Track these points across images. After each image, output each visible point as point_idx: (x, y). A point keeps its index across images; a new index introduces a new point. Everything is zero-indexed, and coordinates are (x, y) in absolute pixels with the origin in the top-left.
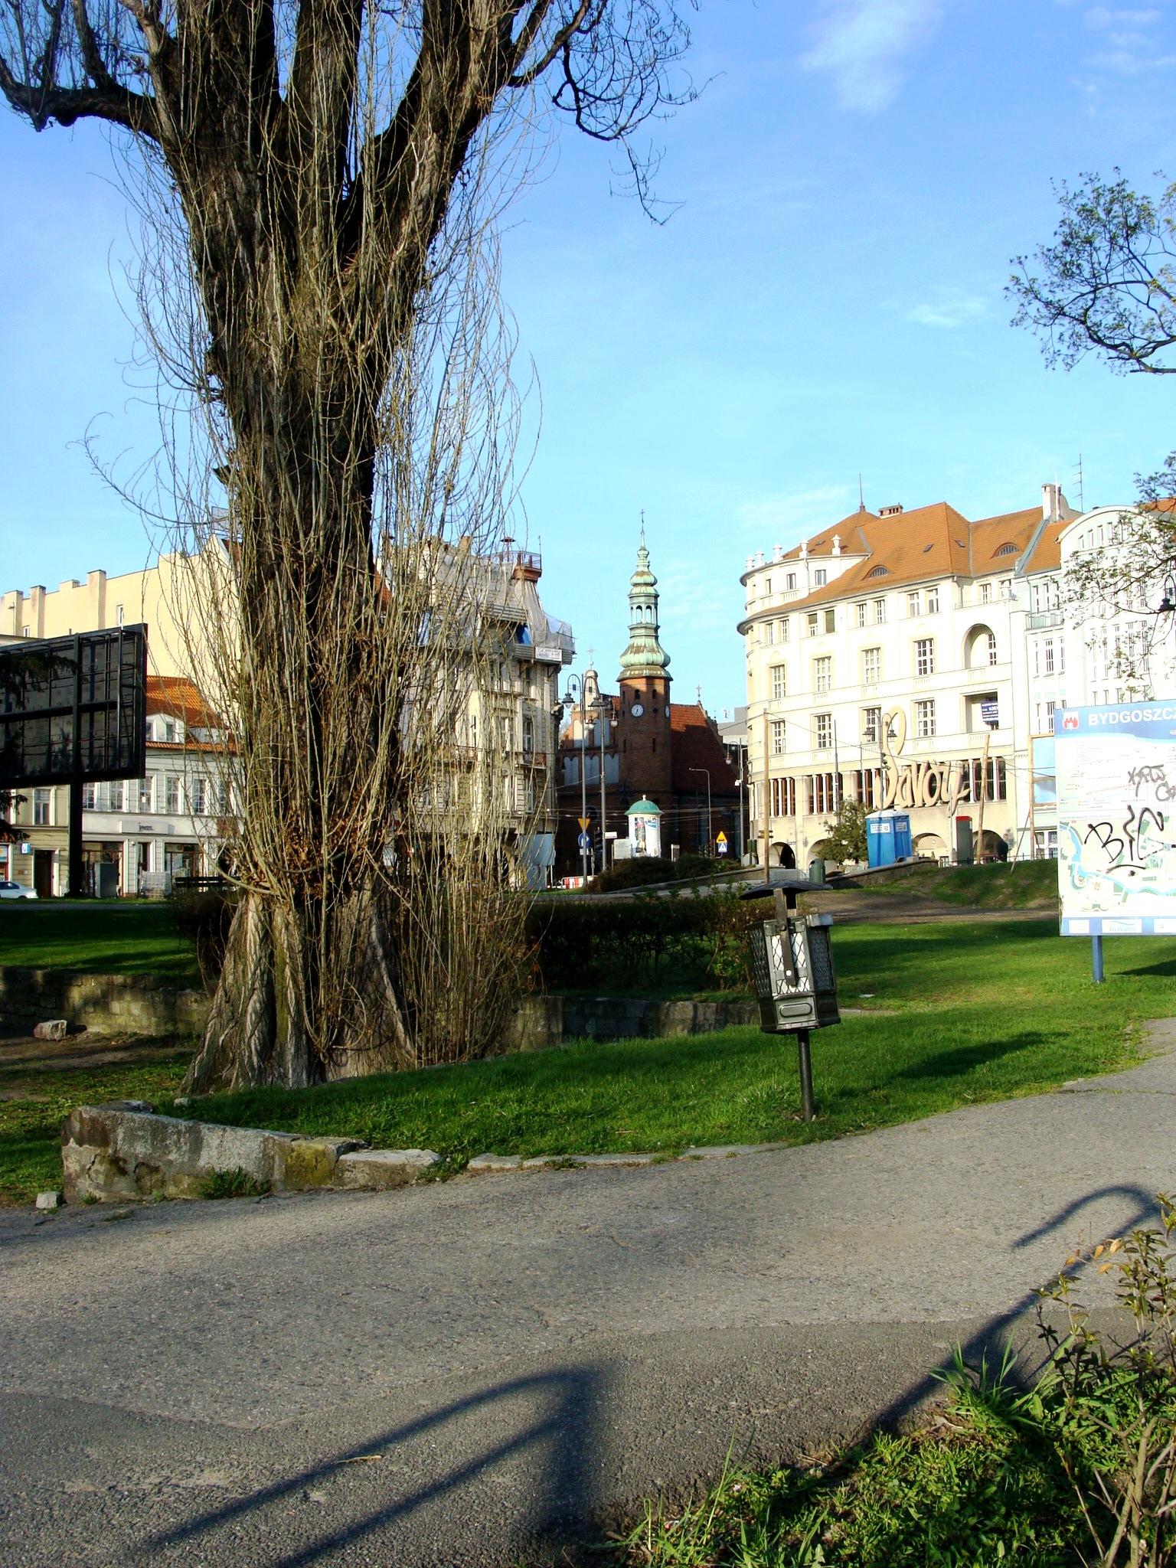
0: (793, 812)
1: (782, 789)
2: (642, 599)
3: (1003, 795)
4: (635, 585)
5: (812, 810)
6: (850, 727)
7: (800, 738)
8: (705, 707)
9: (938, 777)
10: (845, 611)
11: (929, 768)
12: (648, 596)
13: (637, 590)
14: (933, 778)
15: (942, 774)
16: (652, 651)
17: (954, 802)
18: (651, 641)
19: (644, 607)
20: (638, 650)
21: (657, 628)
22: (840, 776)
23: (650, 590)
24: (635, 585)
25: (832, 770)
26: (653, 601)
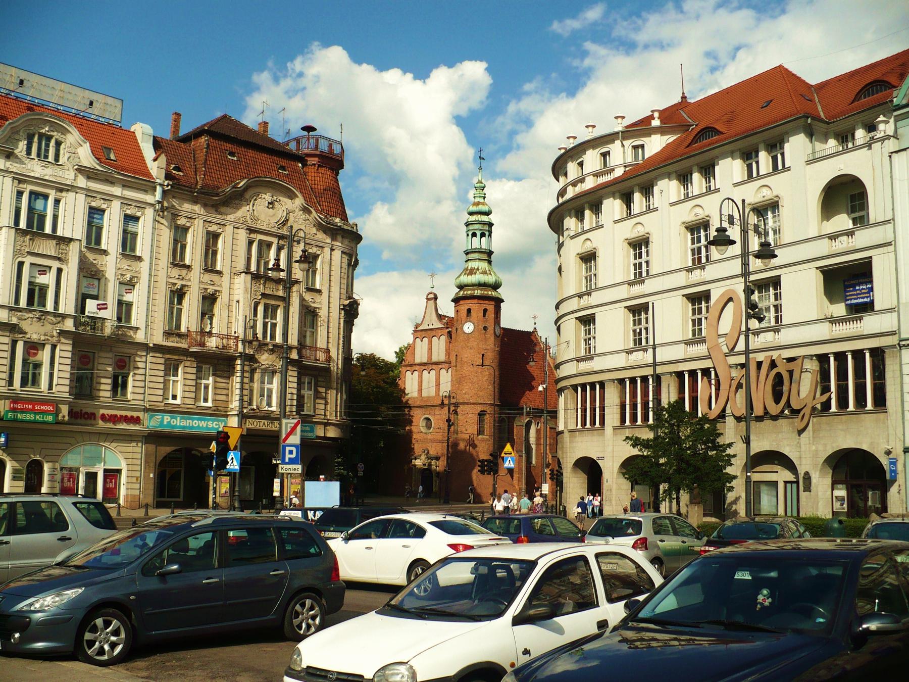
0: (602, 422)
1: (590, 389)
3: (880, 400)
4: (471, 214)
5: (623, 420)
6: (671, 320)
7: (613, 329)
9: (786, 376)
10: (667, 189)
11: (773, 365)
12: (483, 223)
13: (473, 218)
14: (779, 379)
15: (791, 373)
16: (485, 273)
17: (807, 411)
18: (484, 265)
19: (478, 233)
20: (472, 272)
21: (490, 253)
22: (658, 378)
23: (485, 218)
24: (471, 214)
25: (649, 371)
26: (486, 228)
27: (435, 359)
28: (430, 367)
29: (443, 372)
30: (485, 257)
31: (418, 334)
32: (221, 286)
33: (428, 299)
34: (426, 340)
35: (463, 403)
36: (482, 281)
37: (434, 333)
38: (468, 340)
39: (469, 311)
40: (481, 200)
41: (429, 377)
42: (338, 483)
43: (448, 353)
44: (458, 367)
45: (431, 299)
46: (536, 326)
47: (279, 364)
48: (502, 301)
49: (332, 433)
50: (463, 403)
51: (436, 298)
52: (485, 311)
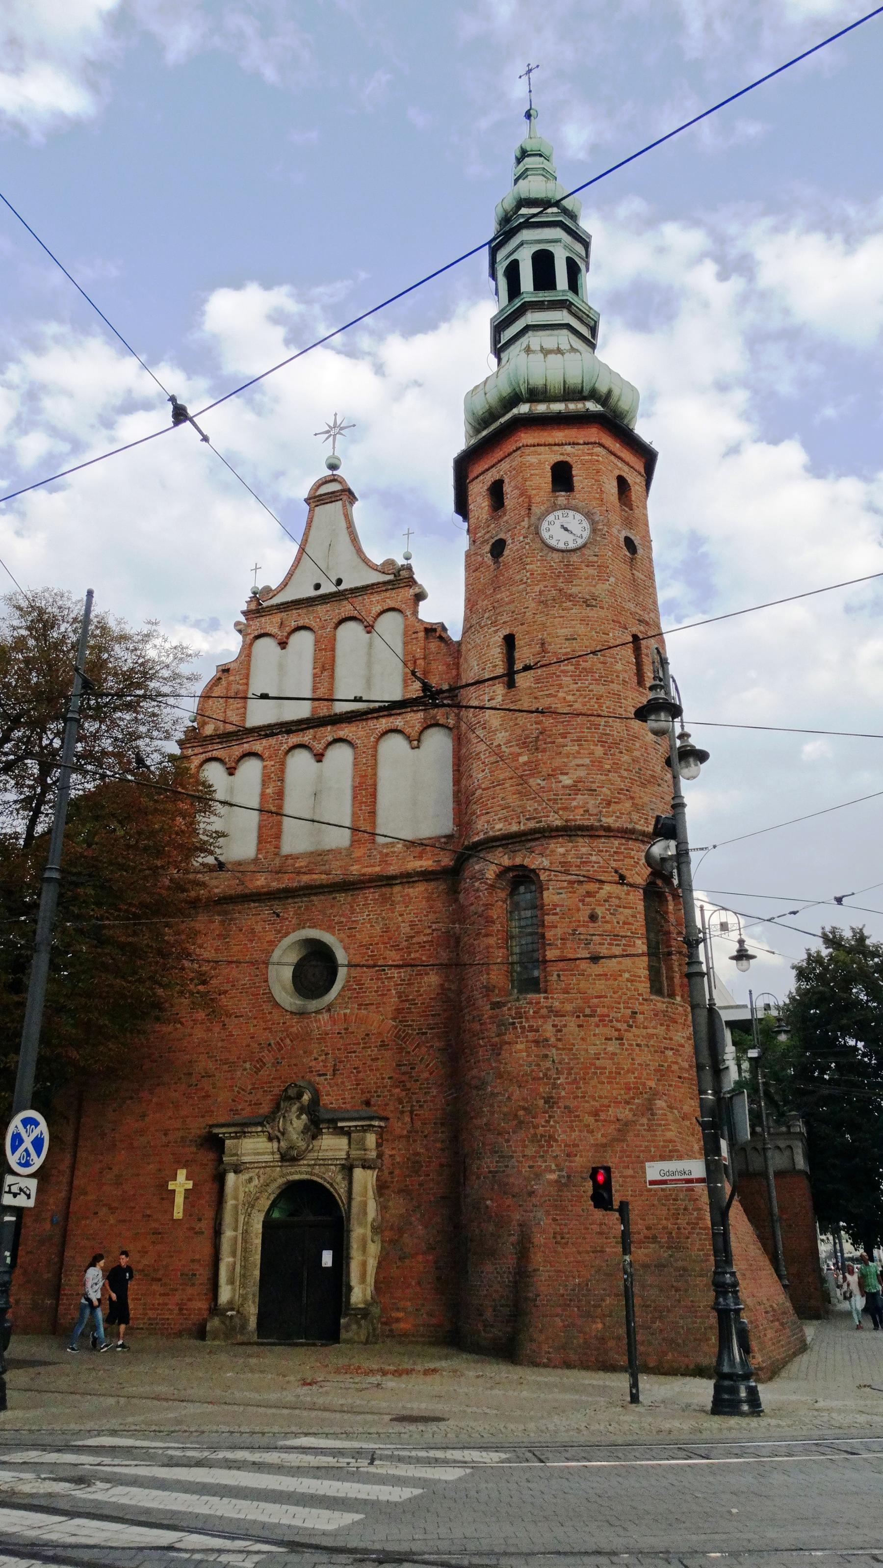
28: (329, 734)
31: (270, 624)
33: (316, 500)
34: (303, 642)
35: (569, 832)
37: (346, 608)
38: (570, 573)
39: (562, 477)
41: (318, 783)
45: (332, 498)
50: (569, 832)
52: (622, 483)
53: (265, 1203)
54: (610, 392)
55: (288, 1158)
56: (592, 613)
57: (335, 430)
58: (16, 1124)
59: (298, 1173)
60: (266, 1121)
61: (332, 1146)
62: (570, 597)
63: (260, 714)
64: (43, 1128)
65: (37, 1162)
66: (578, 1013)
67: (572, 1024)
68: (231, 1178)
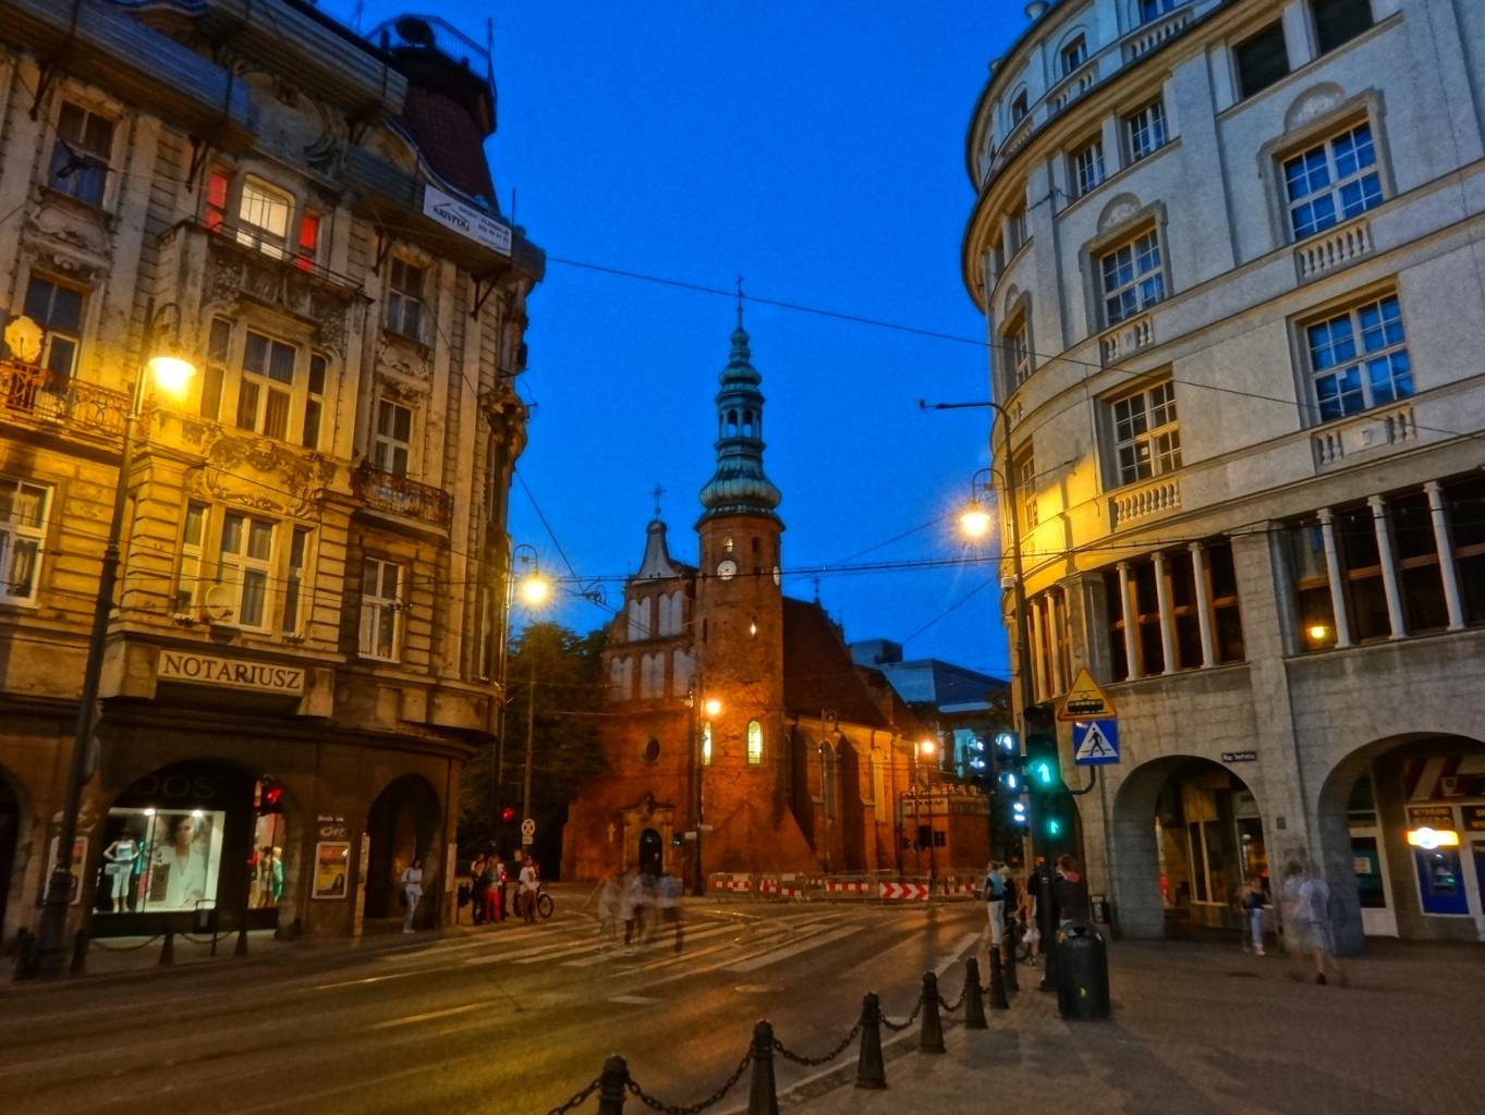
2: (738, 401)
4: (729, 380)
8: (825, 606)
13: (732, 387)
19: (740, 412)
23: (750, 387)
24: (729, 380)
27: (664, 630)
29: (679, 655)
30: (749, 451)
32: (108, 255)
33: (650, 531)
34: (647, 602)
36: (749, 492)
40: (744, 360)
42: (152, 696)
43: (688, 616)
44: (709, 641)
46: (819, 595)
47: (287, 504)
48: (783, 528)
49: (451, 715)
51: (664, 528)
53: (639, 836)
54: (754, 493)
55: (644, 820)
56: (733, 610)
57: (658, 493)
58: (524, 824)
59: (648, 825)
60: (635, 806)
61: (658, 817)
62: (726, 603)
63: (634, 634)
64: (533, 823)
65: (532, 832)
66: (721, 773)
67: (717, 778)
68: (626, 828)
